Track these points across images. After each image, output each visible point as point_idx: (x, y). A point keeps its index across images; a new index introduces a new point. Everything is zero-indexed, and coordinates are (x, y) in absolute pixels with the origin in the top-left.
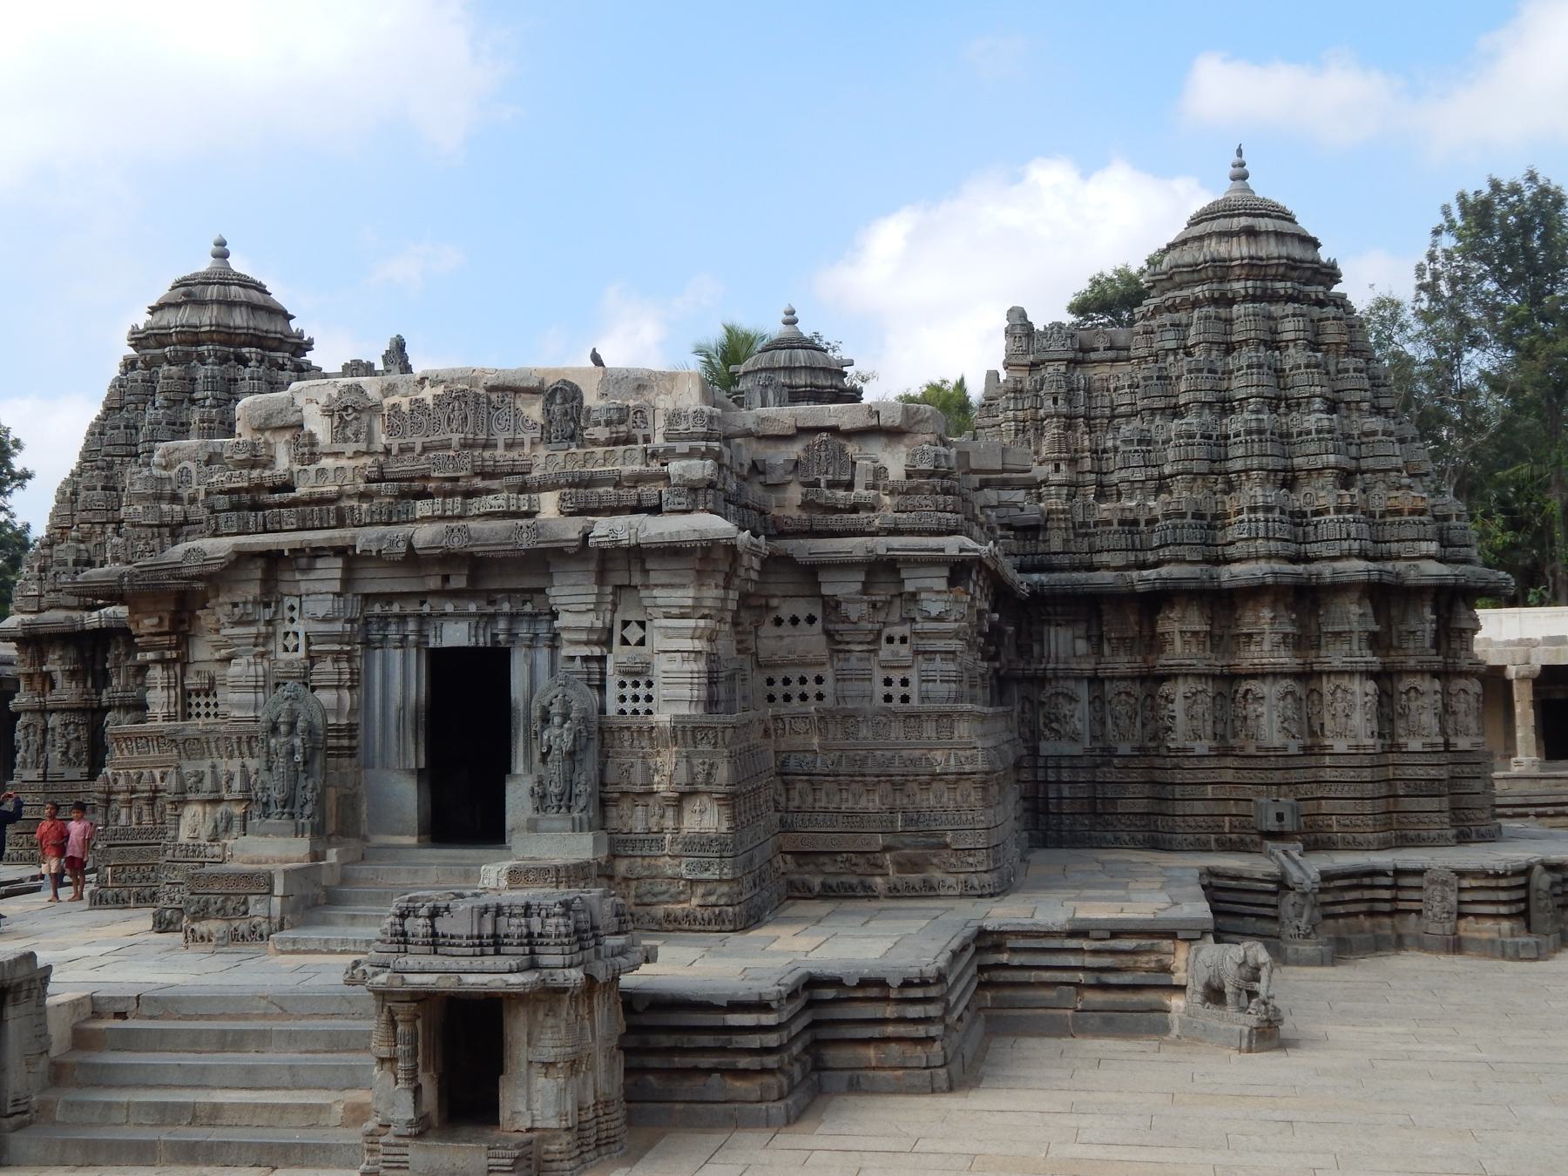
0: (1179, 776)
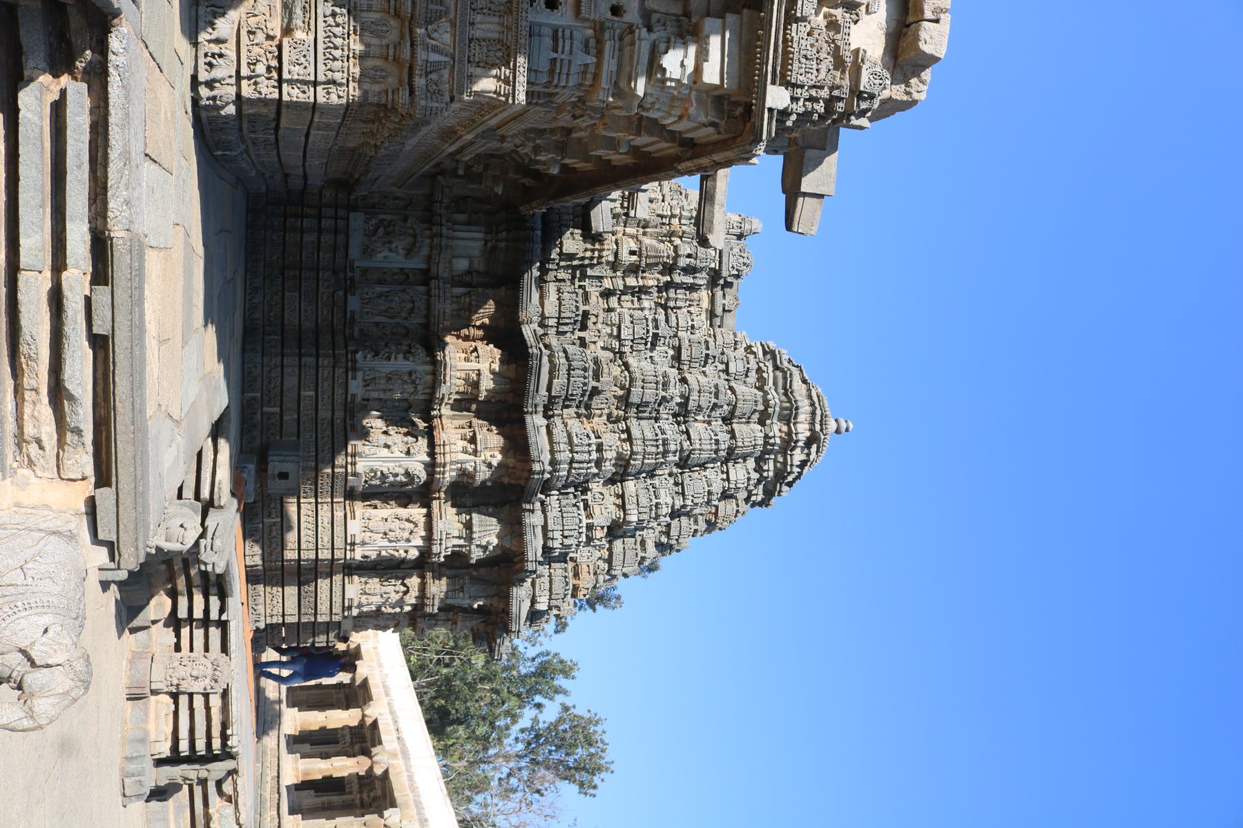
0: (324, 362)
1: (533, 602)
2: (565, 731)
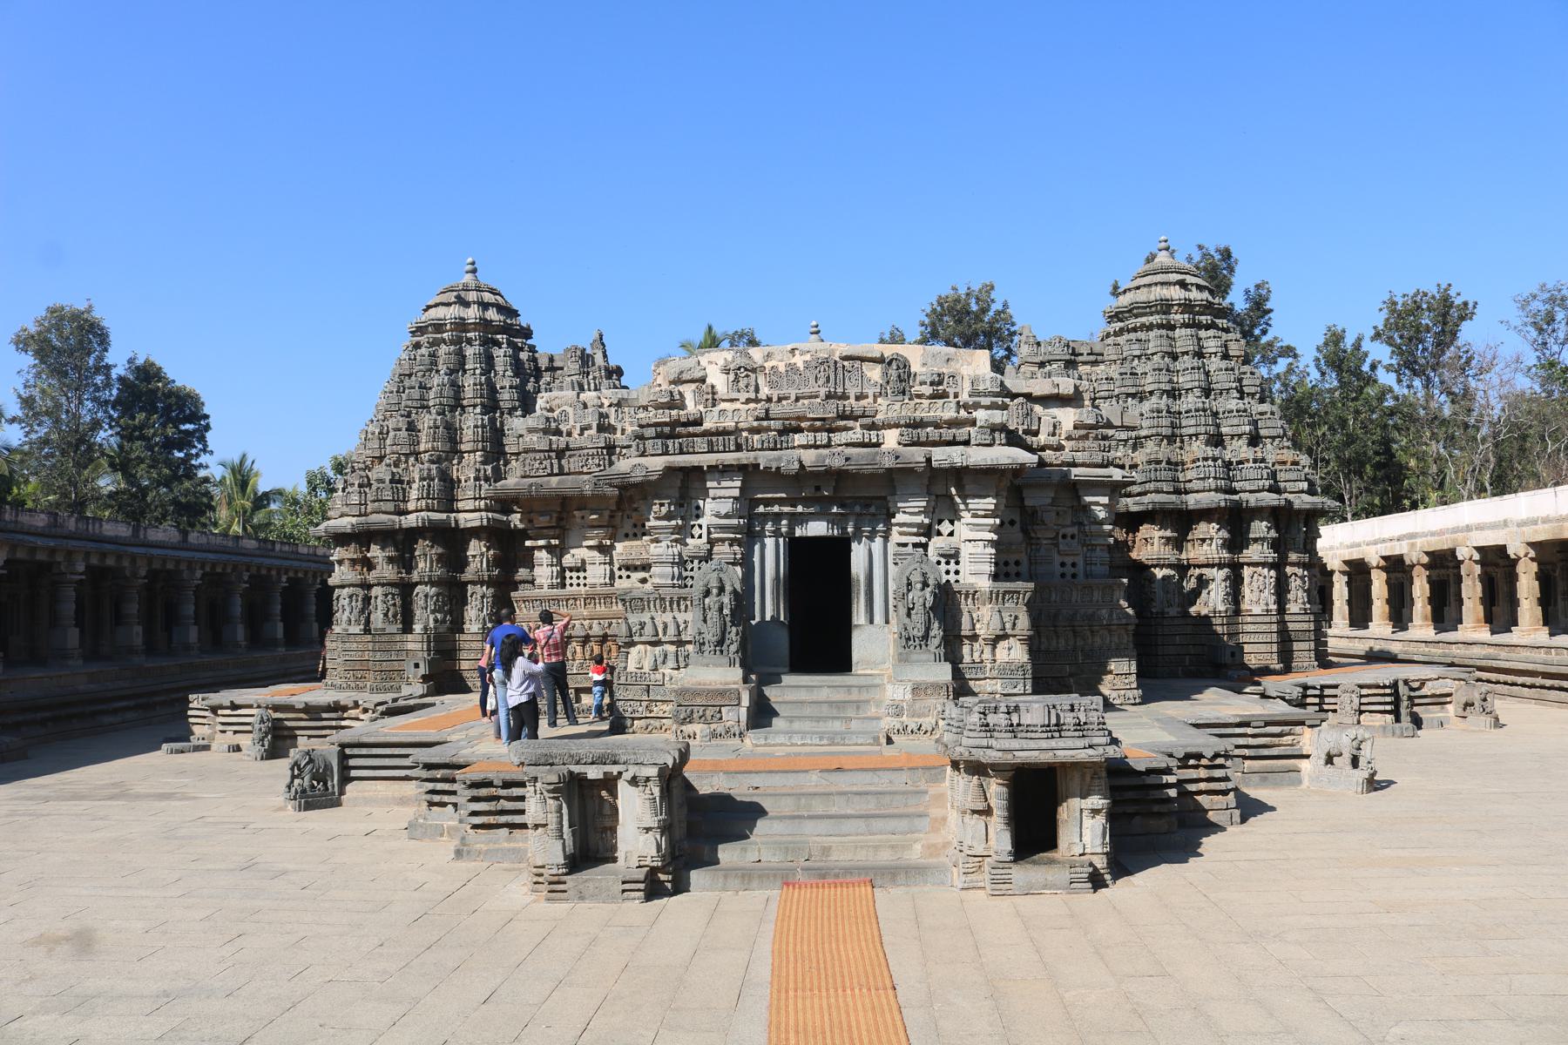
1: (1302, 492)
2: (1401, 337)
